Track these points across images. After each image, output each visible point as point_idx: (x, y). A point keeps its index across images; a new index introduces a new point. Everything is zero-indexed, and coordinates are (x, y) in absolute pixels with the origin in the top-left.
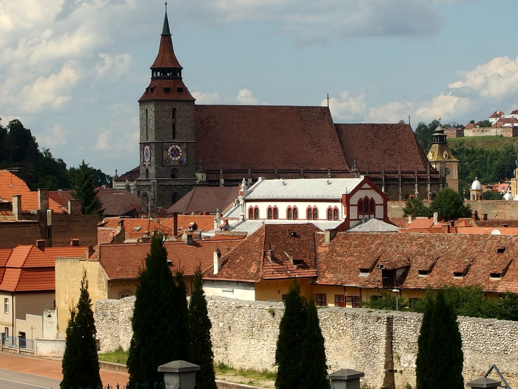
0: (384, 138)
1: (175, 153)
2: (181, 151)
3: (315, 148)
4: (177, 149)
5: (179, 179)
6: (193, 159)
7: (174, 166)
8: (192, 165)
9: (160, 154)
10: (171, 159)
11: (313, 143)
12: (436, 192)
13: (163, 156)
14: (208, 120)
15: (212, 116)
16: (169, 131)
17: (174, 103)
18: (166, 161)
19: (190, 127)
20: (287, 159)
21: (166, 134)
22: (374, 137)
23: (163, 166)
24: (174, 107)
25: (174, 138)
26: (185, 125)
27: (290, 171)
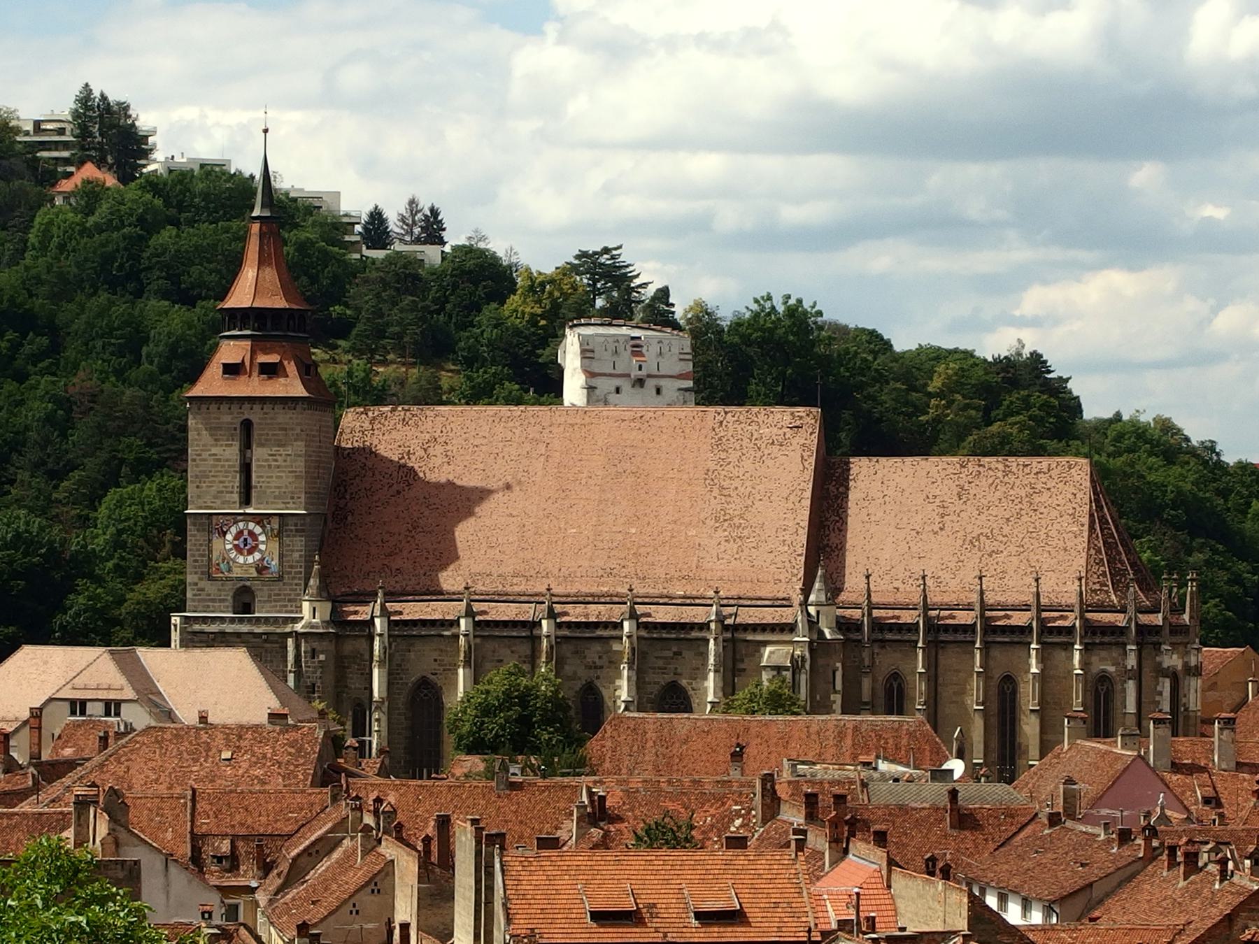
0: (986, 502)
1: (247, 544)
2: (262, 538)
3: (725, 530)
4: (251, 533)
5: (257, 615)
6: (297, 562)
7: (241, 579)
8: (294, 578)
9: (201, 545)
10: (234, 561)
11: (724, 515)
12: (1112, 669)
13: (210, 551)
14: (425, 450)
15: (444, 439)
16: (229, 482)
17: (247, 406)
18: (218, 564)
19: (290, 472)
20: (620, 562)
21: (222, 492)
22: (956, 497)
23: (210, 578)
24: (246, 416)
25: (246, 501)
26: (278, 467)
27: (608, 599)
